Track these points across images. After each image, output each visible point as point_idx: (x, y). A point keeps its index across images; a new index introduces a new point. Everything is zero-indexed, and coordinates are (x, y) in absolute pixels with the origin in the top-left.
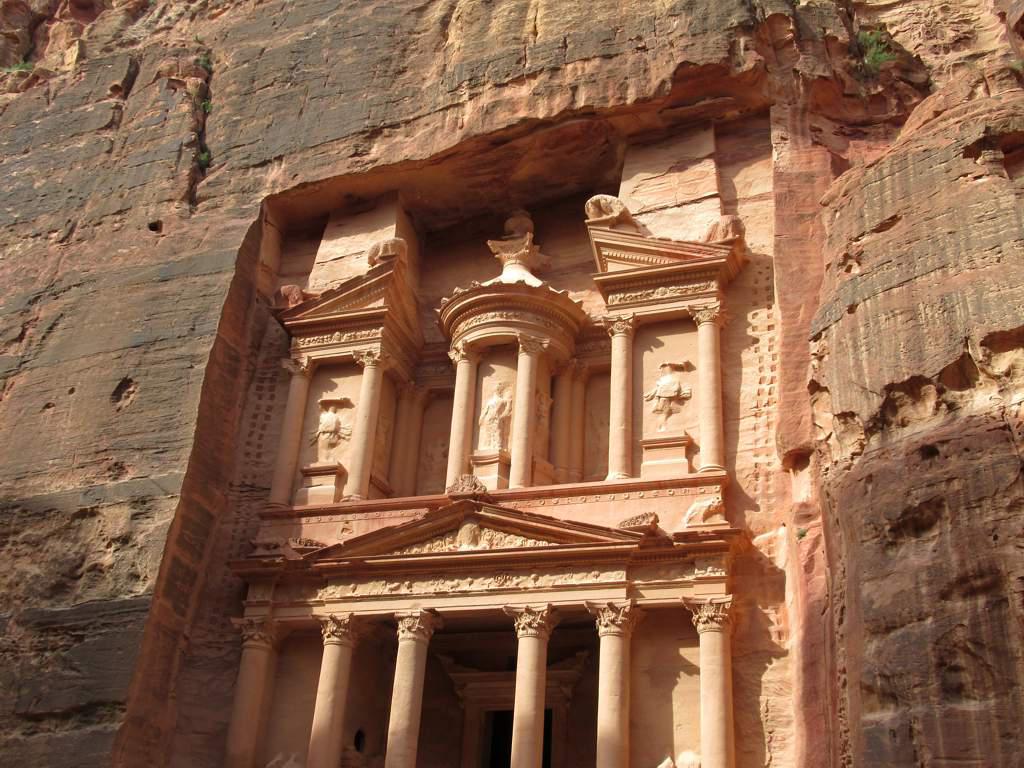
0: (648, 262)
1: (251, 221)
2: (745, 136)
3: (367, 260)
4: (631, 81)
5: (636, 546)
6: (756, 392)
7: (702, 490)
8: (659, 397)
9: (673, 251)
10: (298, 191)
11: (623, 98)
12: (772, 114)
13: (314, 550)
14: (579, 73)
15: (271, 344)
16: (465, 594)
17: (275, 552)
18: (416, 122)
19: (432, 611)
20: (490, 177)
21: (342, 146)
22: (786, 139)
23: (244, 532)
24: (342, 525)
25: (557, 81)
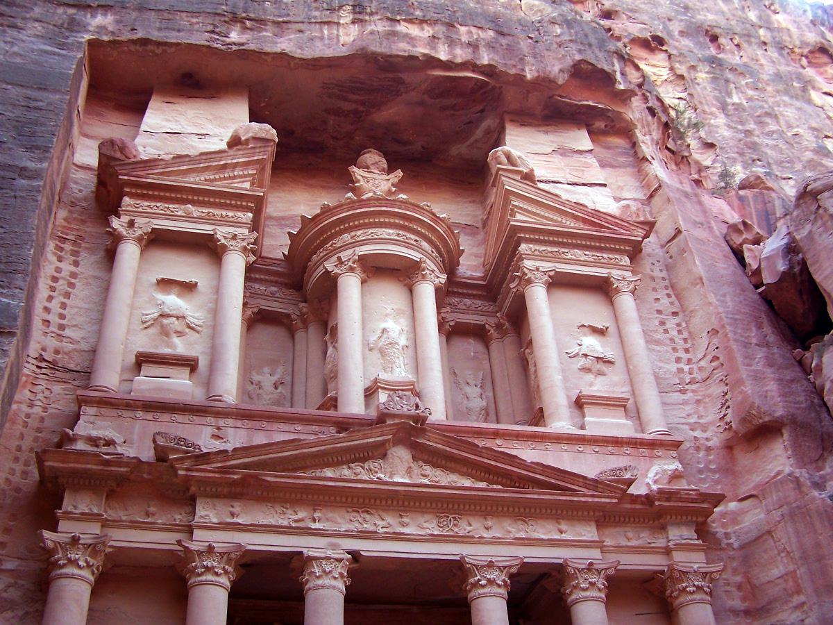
0: (561, 222)
1: (80, 55)
2: (609, 148)
3: (227, 138)
4: (530, 59)
5: (616, 501)
7: (660, 454)
8: (586, 355)
9: (589, 218)
10: (133, 48)
11: (523, 70)
13: (187, 452)
15: (73, 204)
17: (105, 449)
18: (284, 25)
19: (355, 556)
20: (354, 106)
21: (194, 20)
23: (42, 419)
24: (209, 431)
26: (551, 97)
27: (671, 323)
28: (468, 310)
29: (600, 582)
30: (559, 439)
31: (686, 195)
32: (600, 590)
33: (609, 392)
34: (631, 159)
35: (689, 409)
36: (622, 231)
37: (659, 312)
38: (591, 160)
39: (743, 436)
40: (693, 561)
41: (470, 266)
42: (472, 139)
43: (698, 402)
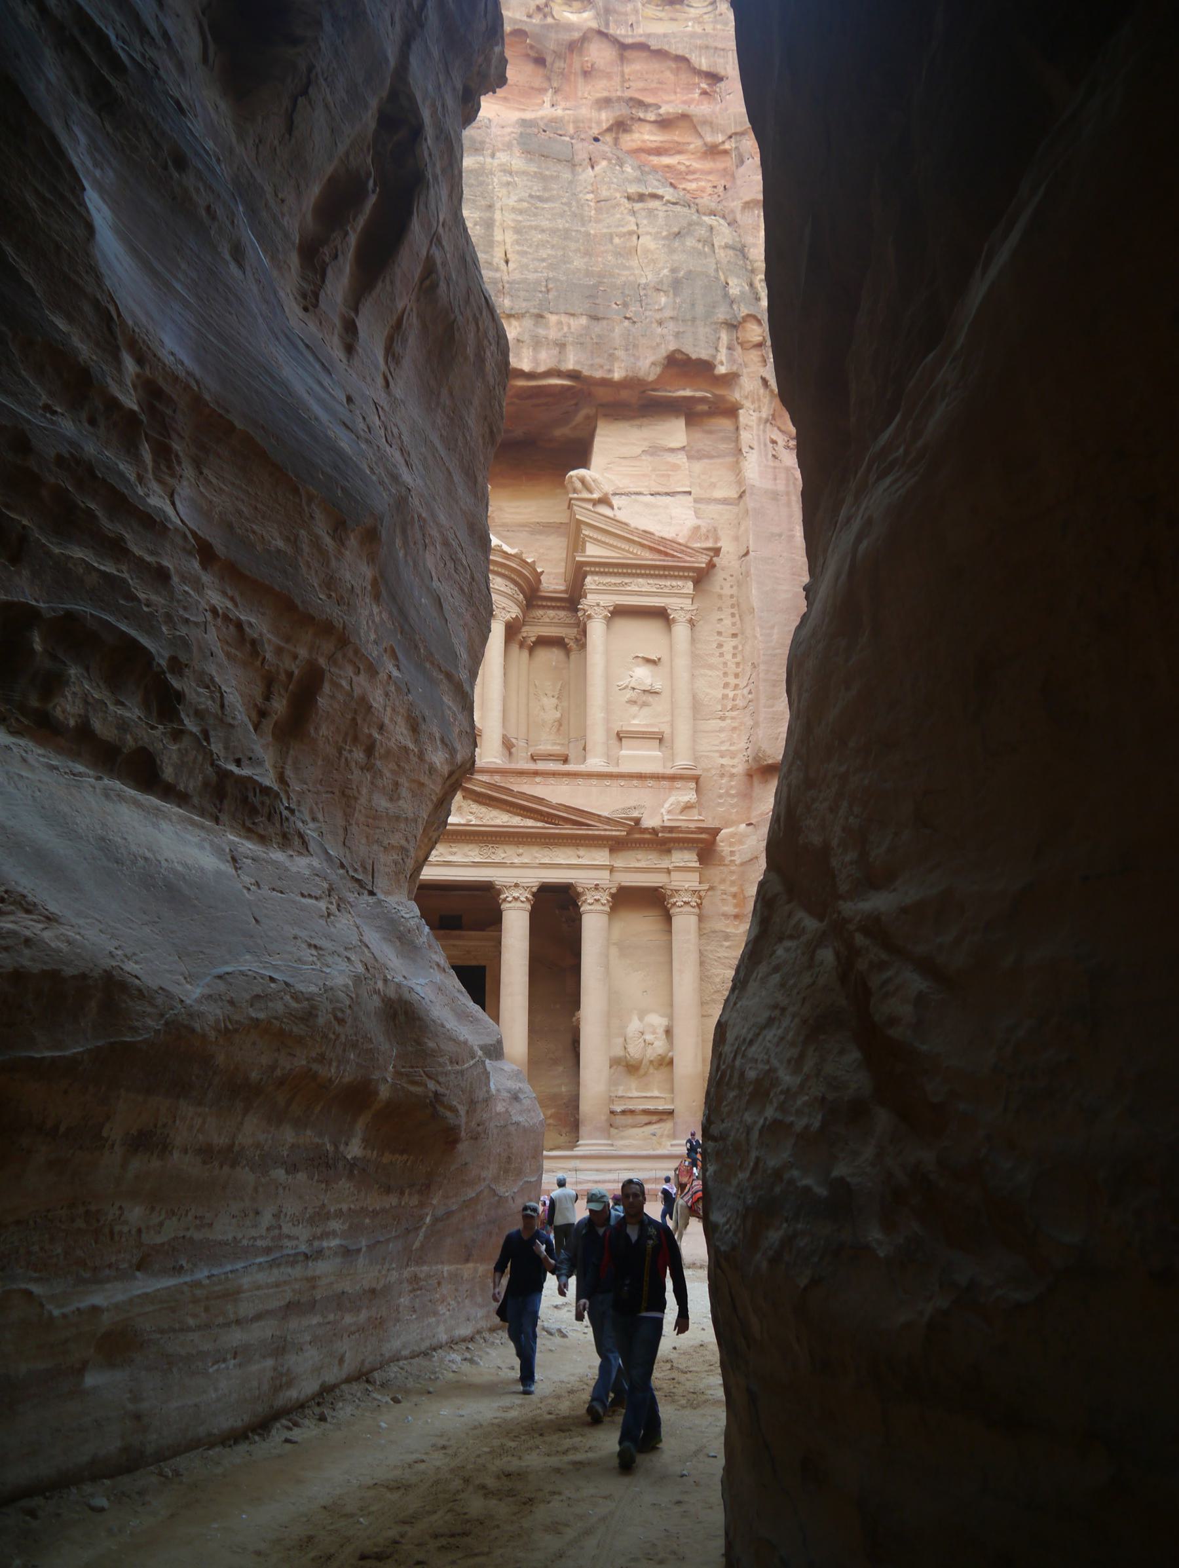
0: (628, 551)
2: (710, 432)
4: (620, 353)
6: (720, 696)
11: (610, 371)
12: (741, 419)
14: (566, 329)
16: (448, 864)
22: (751, 448)
25: (541, 332)
26: (644, 392)
27: (729, 644)
28: (550, 624)
29: (605, 898)
30: (590, 775)
31: (774, 496)
32: (603, 905)
33: (647, 725)
34: (732, 445)
35: (722, 735)
36: (689, 559)
37: (719, 633)
38: (681, 459)
39: (757, 769)
40: (691, 881)
41: (553, 582)
42: (574, 423)
43: (734, 729)
